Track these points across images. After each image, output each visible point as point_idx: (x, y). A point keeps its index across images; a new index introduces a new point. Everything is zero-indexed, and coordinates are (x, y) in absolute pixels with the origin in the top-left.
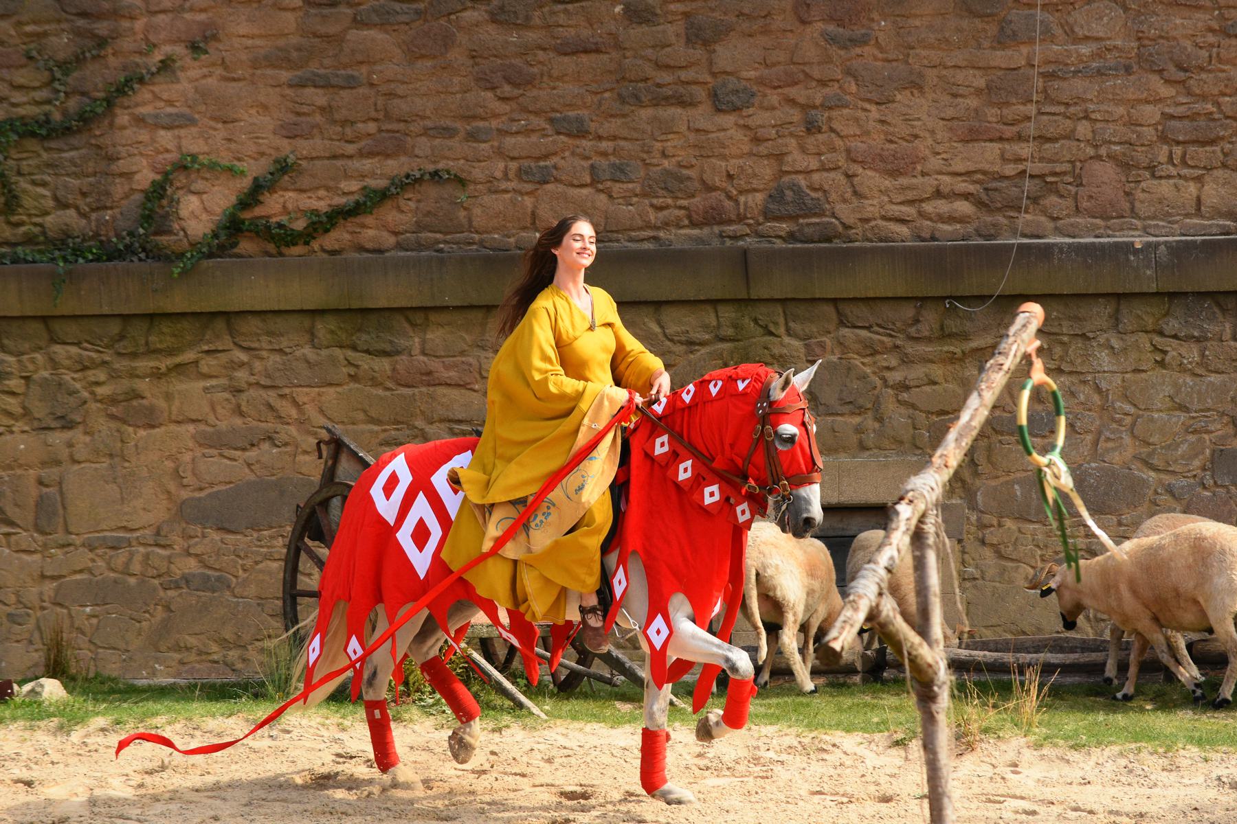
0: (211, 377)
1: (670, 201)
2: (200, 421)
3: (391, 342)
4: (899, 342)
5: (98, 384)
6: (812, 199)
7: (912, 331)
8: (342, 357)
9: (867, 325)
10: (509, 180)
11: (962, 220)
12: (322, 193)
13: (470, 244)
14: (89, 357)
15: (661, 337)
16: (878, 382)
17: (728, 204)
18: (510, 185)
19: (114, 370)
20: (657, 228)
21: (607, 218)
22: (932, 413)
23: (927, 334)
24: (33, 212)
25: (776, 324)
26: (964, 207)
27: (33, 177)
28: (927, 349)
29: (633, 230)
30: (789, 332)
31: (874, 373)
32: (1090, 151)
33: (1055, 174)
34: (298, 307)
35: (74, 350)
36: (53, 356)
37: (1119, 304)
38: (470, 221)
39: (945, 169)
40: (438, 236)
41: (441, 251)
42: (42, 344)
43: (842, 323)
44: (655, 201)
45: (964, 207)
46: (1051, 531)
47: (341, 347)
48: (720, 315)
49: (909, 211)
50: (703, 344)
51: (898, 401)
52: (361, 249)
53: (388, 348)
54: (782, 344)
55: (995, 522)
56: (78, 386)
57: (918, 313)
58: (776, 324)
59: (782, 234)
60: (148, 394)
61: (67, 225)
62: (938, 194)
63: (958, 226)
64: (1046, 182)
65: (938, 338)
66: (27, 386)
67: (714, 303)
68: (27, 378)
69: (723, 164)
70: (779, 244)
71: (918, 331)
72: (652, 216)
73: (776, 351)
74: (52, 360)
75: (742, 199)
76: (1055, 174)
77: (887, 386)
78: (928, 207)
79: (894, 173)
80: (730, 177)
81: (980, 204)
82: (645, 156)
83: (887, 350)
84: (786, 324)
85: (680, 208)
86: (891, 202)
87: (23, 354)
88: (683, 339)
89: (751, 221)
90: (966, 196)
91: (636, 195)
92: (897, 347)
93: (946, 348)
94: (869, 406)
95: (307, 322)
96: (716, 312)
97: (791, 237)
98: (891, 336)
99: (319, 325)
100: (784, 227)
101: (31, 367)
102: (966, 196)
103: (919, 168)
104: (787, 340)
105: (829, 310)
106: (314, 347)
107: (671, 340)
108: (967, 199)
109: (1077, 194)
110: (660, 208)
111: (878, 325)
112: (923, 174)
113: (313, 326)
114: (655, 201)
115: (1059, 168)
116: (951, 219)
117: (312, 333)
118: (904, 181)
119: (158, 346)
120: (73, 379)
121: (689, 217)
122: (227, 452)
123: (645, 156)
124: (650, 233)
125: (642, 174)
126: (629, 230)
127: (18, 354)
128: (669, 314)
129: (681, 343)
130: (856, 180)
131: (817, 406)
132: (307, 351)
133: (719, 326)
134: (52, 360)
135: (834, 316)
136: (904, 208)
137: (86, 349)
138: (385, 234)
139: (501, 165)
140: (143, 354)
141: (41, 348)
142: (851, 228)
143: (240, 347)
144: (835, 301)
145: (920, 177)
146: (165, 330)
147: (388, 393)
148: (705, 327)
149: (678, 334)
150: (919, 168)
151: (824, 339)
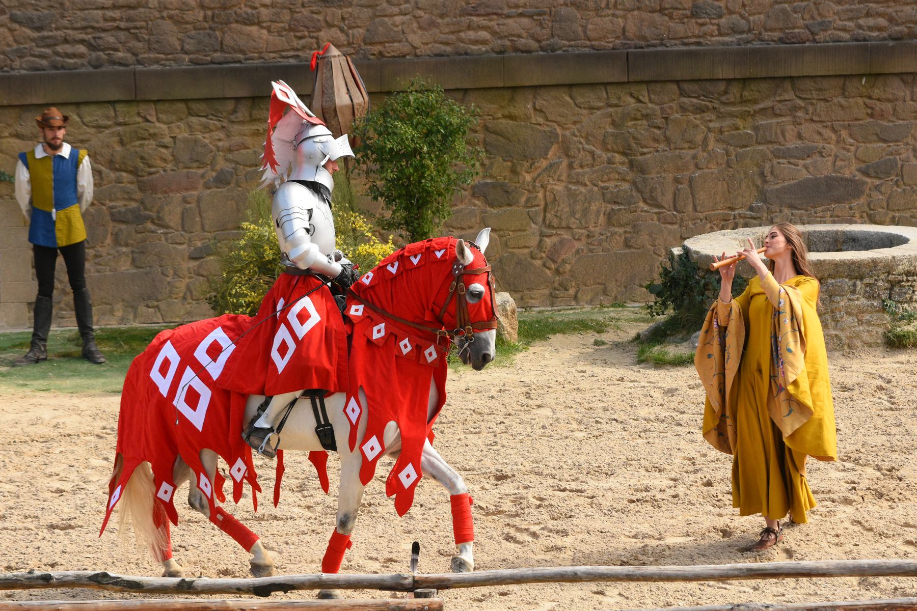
0: (781, 116)
1: (708, 20)
2: (775, 142)
3: (893, 94)
4: (224, 124)
5: (710, 121)
6: (395, 32)
7: (233, 117)
8: (862, 104)
9: (697, 95)
10: (609, 9)
11: (81, 56)
12: (90, 30)
13: (585, 47)
14: (705, 105)
15: (81, 124)
16: (214, 149)
17: (743, 22)
18: (610, 12)
19: (721, 113)
20: (297, 50)
21: (267, 44)
22: (247, 166)
23: (242, 119)
24: (312, 30)
25: (644, 96)
26: (82, 49)
27: (311, 8)
28: (733, 109)
29: (284, 51)
30: (158, 120)
31: (211, 143)
32: (157, 14)
33: (136, 28)
34: (180, 98)
35: (204, 120)
36: (190, 124)
37: (845, 81)
38: (585, 32)
39: (69, 26)
40: (162, 56)
41: (164, 65)
42: (184, 117)
43: (190, 114)
44: (699, 21)
45: (82, 49)
46: (811, 214)
47: (861, 97)
48: (609, 91)
49: (453, 37)
50: (106, 127)
51: (226, 160)
52: (516, 50)
53: (890, 97)
54: (155, 127)
55: (778, 211)
56: (207, 141)
57: (727, 88)
58: (644, 96)
59: (775, 39)
60: (251, 147)
61: (733, 24)
62: (66, 41)
63: (481, 46)
64: (131, 33)
65: (248, 122)
66: (175, 143)
67: (112, 103)
68: (174, 138)
69: (340, 11)
70: (773, 45)
71: (236, 118)
72: (296, 43)
73: (152, 131)
74: (190, 126)
75: (751, 18)
76: (136, 28)
77: (219, 151)
78: (59, 49)
79: (39, 29)
80: (343, 19)
81: (92, 47)
82: (292, 7)
83: (218, 129)
84: (157, 115)
85: (713, 24)
86: (37, 46)
87: (172, 123)
88: (587, 106)
89: (355, 45)
90: (82, 42)
91: (285, 30)
92: (223, 127)
93: (254, 128)
94: (209, 162)
95: (841, 81)
96: (606, 90)
97: (781, 41)
98: (220, 121)
99: (848, 84)
100: (777, 35)
101: (177, 131)
102: (82, 42)
103: (53, 26)
104: (158, 124)
105: (674, 87)
106: (845, 97)
107: (88, 126)
108: (486, 30)
109: (149, 40)
110: (301, 38)
111: (212, 115)
112: (57, 29)
113: (844, 85)
114: (699, 21)
115: (138, 24)
116: (74, 56)
117: (261, 108)
118: (45, 33)
119: (258, 117)
120: (695, 119)
121: (719, 30)
122: (792, 161)
123: (292, 7)
124: (292, 53)
125: (288, 18)
126: (281, 51)
127: (168, 123)
128: (85, 110)
129: (94, 127)
130: (15, 33)
131: (669, 144)
132: (842, 100)
133: (116, 116)
134: (190, 126)
135: (186, 111)
136: (43, 50)
137: (211, 119)
138: (129, 55)
139: (202, 14)
140: (248, 122)
141: (182, 119)
142: (417, 48)
143: (800, 98)
144: (186, 101)
145: (459, 18)
146: (262, 107)
147: (891, 124)
148: (108, 118)
149: (91, 122)
150: (53, 26)
151: (179, 123)
